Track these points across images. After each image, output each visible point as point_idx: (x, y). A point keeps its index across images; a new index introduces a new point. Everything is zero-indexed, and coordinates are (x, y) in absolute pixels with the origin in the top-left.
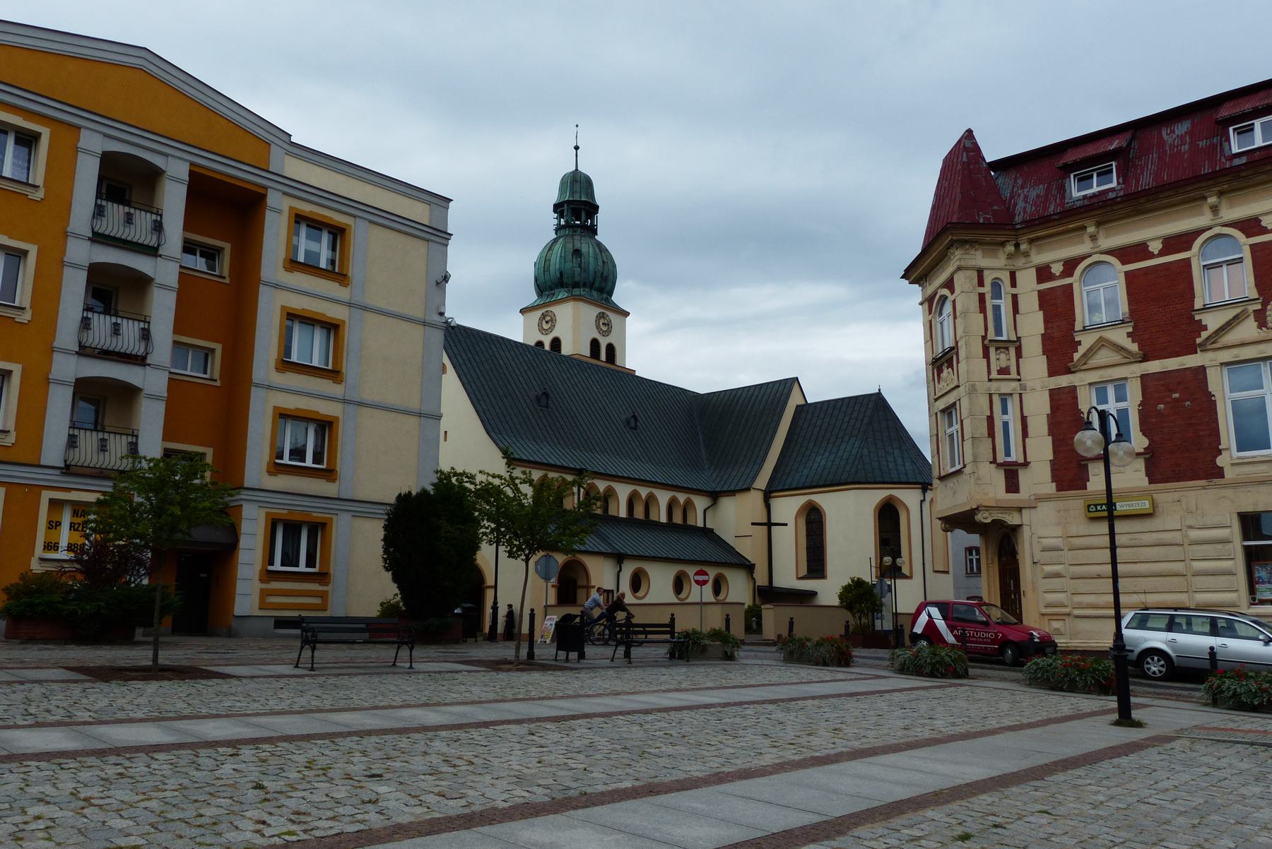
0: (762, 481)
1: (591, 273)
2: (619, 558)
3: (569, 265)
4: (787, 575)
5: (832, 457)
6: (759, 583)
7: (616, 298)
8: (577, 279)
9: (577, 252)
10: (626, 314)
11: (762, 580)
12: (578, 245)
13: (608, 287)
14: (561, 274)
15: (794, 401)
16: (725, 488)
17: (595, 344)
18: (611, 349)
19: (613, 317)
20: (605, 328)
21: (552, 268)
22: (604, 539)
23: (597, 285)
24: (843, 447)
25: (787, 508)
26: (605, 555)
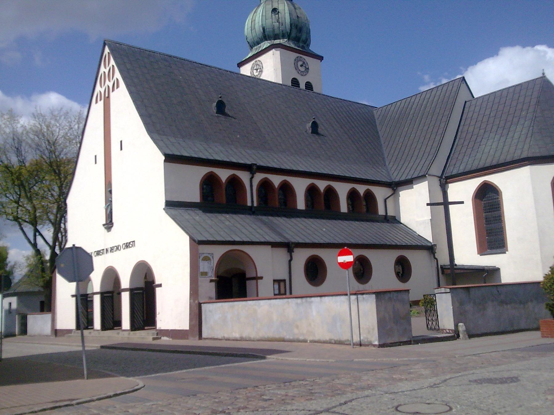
0: (437, 169)
1: (288, 26)
2: (290, 247)
3: (269, 21)
4: (467, 252)
5: (503, 139)
6: (441, 263)
7: (313, 48)
8: (277, 31)
9: (275, 10)
10: (321, 58)
11: (444, 260)
12: (275, 6)
13: (304, 37)
14: (264, 29)
15: (463, 96)
16: (403, 178)
17: (295, 82)
18: (309, 86)
19: (308, 59)
20: (302, 69)
21: (257, 26)
22: (273, 229)
23: (293, 35)
24: (513, 128)
25: (463, 191)
26: (274, 245)
